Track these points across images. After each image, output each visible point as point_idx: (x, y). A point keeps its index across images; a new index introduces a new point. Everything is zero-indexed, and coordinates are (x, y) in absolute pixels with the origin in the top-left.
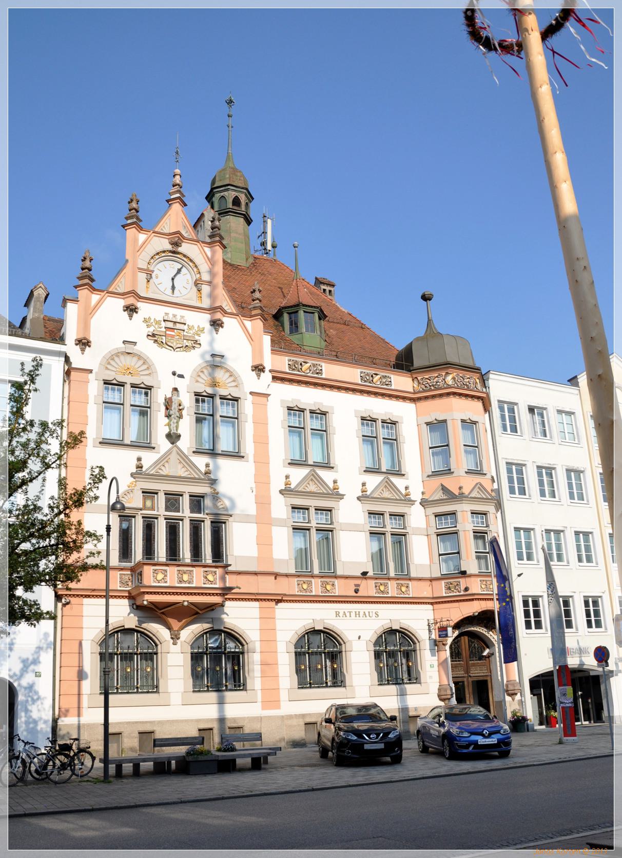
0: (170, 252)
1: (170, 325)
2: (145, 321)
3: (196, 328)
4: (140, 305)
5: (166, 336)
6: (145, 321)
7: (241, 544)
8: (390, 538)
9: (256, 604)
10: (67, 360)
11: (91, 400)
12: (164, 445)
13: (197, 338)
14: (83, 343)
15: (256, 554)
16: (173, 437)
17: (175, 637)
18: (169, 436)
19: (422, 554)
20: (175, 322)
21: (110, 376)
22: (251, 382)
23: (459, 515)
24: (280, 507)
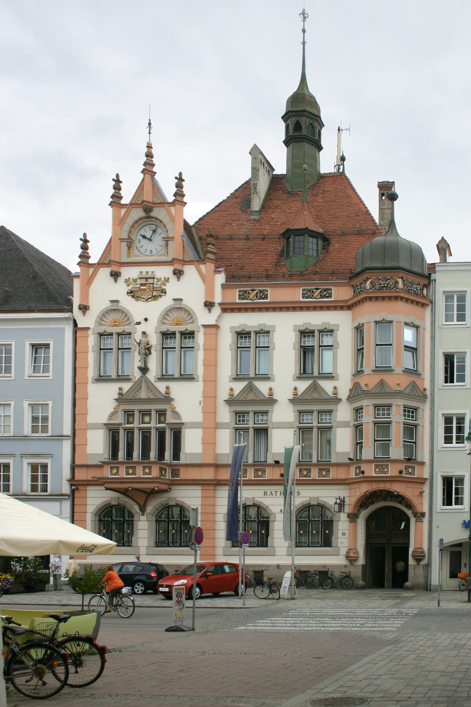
0: (146, 218)
1: (143, 281)
3: (163, 279)
7: (192, 444)
9: (199, 487)
13: (163, 287)
15: (201, 451)
17: (143, 510)
18: (140, 368)
20: (146, 279)
24: (225, 415)
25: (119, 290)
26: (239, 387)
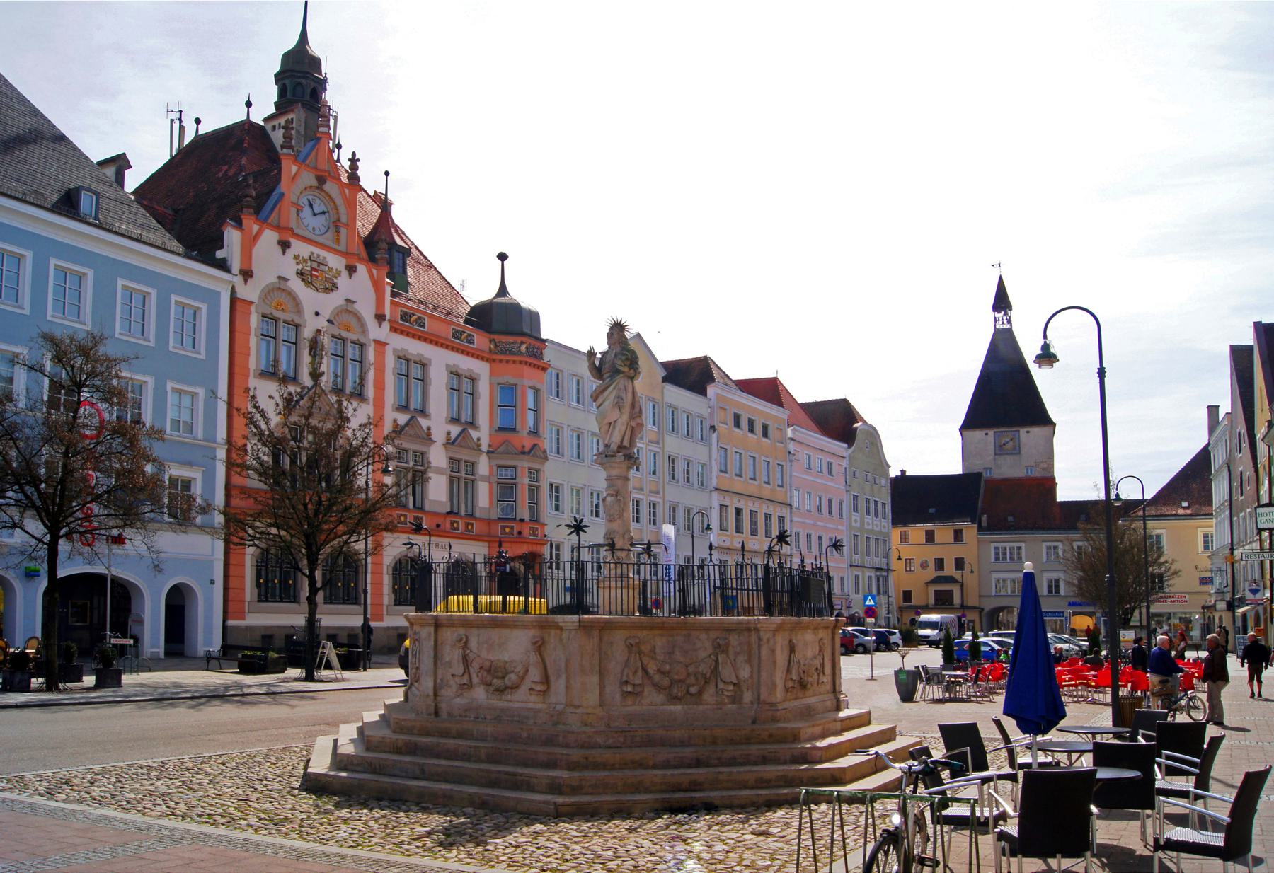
1: (315, 265)
2: (296, 257)
4: (294, 242)
5: (312, 275)
6: (296, 257)
8: (461, 478)
10: (233, 292)
11: (253, 332)
12: (308, 382)
14: (247, 274)
16: (316, 375)
19: (484, 496)
20: (319, 264)
21: (267, 311)
22: (379, 332)
23: (519, 470)
25: (288, 267)
26: (403, 419)
